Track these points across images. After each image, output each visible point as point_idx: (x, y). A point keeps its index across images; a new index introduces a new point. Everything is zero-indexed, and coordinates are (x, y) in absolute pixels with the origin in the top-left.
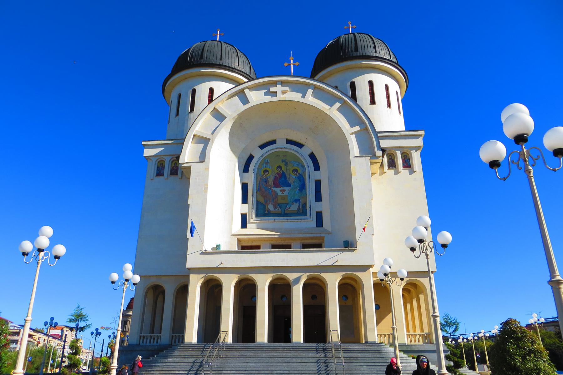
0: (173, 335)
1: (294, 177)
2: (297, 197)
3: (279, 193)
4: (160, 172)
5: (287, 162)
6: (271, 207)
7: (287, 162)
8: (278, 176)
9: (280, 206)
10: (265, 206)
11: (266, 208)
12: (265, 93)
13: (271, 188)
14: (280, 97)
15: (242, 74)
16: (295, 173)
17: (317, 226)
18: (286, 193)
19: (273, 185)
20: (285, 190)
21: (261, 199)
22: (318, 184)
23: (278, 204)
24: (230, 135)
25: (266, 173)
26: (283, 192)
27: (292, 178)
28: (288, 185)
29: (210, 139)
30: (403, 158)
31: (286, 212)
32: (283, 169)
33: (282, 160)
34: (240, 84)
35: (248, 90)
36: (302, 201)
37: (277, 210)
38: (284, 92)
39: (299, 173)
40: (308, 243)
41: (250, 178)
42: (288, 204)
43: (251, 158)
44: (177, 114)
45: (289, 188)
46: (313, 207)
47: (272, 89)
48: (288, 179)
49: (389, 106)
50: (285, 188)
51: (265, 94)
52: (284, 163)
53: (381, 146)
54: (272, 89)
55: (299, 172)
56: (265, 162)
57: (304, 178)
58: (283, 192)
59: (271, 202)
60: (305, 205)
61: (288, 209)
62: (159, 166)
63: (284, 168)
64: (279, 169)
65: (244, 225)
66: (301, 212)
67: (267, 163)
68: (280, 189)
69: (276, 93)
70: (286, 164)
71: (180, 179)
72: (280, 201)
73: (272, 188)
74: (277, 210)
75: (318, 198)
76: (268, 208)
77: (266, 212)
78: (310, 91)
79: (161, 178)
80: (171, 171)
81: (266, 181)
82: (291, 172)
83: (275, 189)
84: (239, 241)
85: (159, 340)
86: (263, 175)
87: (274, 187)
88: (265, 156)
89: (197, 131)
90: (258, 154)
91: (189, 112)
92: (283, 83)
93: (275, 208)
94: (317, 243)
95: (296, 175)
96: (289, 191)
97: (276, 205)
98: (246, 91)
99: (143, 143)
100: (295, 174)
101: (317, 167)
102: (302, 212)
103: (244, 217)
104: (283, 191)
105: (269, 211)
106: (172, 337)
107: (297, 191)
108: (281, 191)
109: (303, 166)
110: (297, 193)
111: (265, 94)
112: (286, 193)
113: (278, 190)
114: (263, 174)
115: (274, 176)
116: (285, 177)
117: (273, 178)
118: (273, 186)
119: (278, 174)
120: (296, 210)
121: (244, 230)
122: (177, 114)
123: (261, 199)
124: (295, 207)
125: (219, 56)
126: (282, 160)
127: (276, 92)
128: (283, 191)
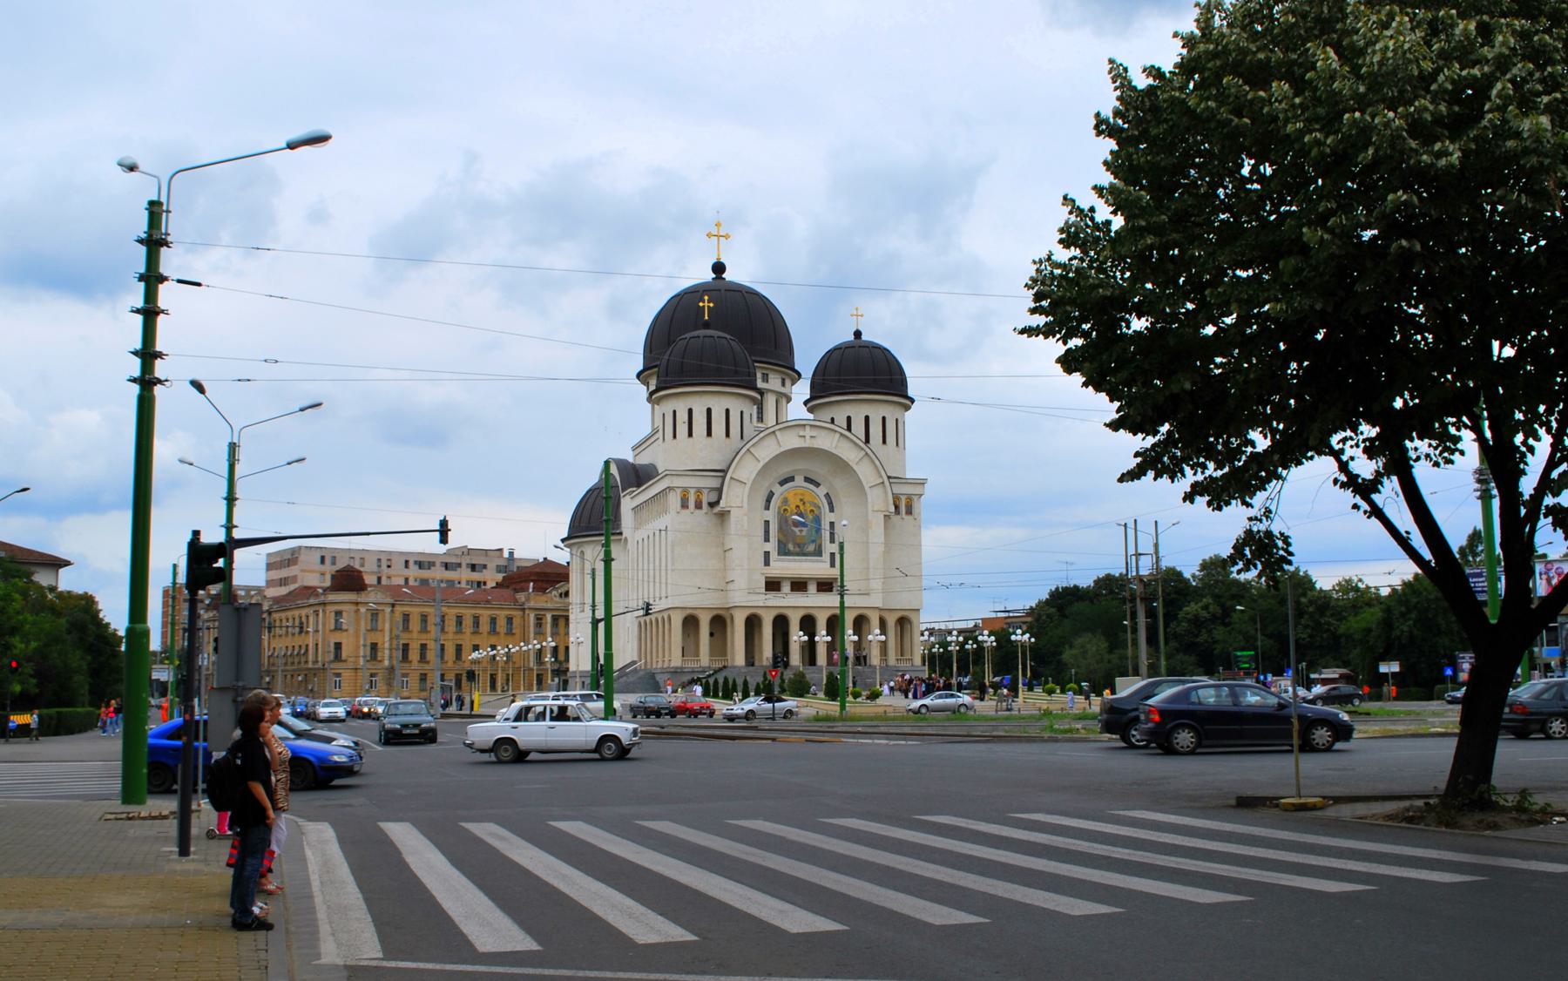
2: (813, 538)
3: (798, 533)
4: (684, 505)
6: (791, 547)
9: (799, 545)
18: (804, 533)
21: (782, 539)
36: (818, 542)
41: (771, 515)
60: (820, 546)
63: (802, 508)
65: (767, 563)
68: (799, 529)
72: (798, 541)
101: (832, 510)
103: (767, 554)
104: (801, 531)
105: (789, 550)
107: (814, 533)
109: (820, 508)
112: (804, 533)
123: (782, 539)
124: (811, 548)
128: (801, 531)
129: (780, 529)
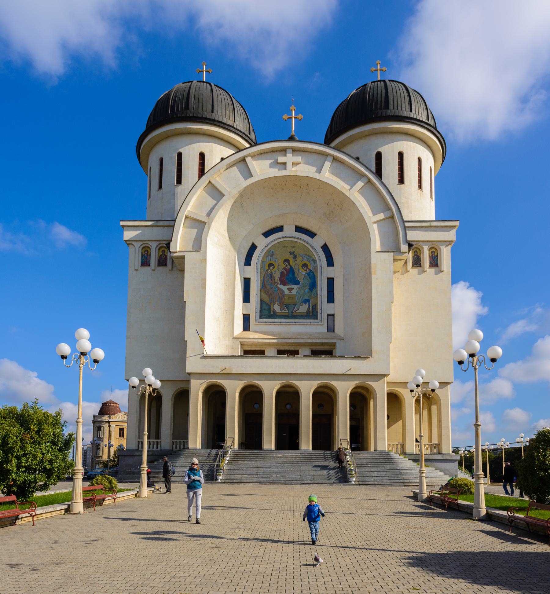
0: (173, 440)
1: (304, 273)
2: (306, 297)
3: (287, 292)
4: (145, 262)
5: (296, 255)
6: (277, 308)
7: (296, 255)
8: (285, 271)
10: (270, 307)
11: (272, 308)
12: (270, 164)
13: (276, 286)
14: (291, 171)
15: (240, 134)
16: (305, 268)
17: (328, 331)
18: (294, 292)
19: (279, 282)
20: (293, 289)
21: (266, 299)
22: (331, 281)
23: (285, 305)
24: (228, 218)
25: (271, 268)
26: (290, 291)
27: (301, 274)
28: (297, 283)
29: (205, 223)
30: (431, 255)
31: (294, 314)
32: (291, 264)
33: (290, 252)
34: (240, 150)
35: (250, 158)
37: (283, 311)
38: (295, 164)
39: (309, 269)
40: (317, 349)
41: (252, 272)
42: (296, 305)
43: (253, 248)
44: (160, 187)
45: (298, 286)
46: (325, 308)
47: (281, 159)
48: (296, 275)
49: (420, 187)
50: (293, 286)
51: (271, 166)
52: (292, 256)
53: (408, 239)
54: (281, 159)
55: (309, 267)
56: (270, 253)
57: (315, 275)
58: (290, 291)
59: (277, 302)
60: (315, 306)
61: (297, 311)
62: (144, 253)
63: (292, 262)
64: (287, 263)
65: (246, 327)
66: (311, 314)
67: (272, 256)
69: (286, 164)
70: (295, 257)
71: (170, 270)
72: (287, 301)
73: (278, 286)
74: (283, 311)
75: (331, 299)
76: (273, 309)
77: (272, 313)
78: (328, 164)
79: (146, 269)
80: (159, 260)
81: (272, 277)
82: (300, 267)
83: (281, 287)
84: (242, 345)
85: (159, 446)
86: (268, 270)
87: (280, 285)
88: (270, 246)
89: (189, 211)
90: (262, 243)
91: (176, 184)
92: (295, 151)
93: (281, 309)
94: (328, 349)
95: (306, 271)
96: (297, 290)
97: (283, 305)
98: (248, 160)
99: (122, 223)
100: (305, 270)
101: (330, 262)
102: (312, 314)
103: (246, 318)
104: (290, 289)
105: (274, 312)
106: (173, 442)
107: (307, 290)
108: (288, 289)
109: (314, 261)
110: (306, 292)
111: (271, 166)
112: (294, 292)
113: (285, 288)
114: (268, 268)
115: (280, 271)
116: (293, 273)
117: (279, 274)
118: (279, 284)
119: (285, 268)
120: (306, 312)
121: (246, 333)
122: (160, 187)
123: (266, 299)
124: (303, 309)
125: (210, 107)
126: (290, 252)
127: (285, 164)
128: (290, 289)
129: (263, 287)
